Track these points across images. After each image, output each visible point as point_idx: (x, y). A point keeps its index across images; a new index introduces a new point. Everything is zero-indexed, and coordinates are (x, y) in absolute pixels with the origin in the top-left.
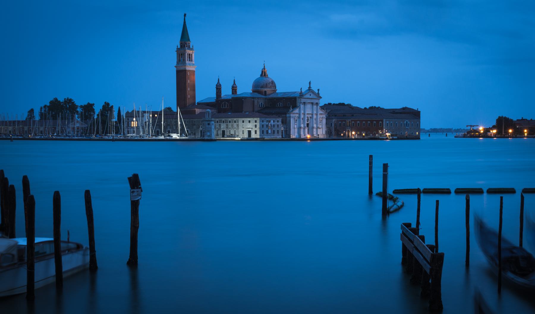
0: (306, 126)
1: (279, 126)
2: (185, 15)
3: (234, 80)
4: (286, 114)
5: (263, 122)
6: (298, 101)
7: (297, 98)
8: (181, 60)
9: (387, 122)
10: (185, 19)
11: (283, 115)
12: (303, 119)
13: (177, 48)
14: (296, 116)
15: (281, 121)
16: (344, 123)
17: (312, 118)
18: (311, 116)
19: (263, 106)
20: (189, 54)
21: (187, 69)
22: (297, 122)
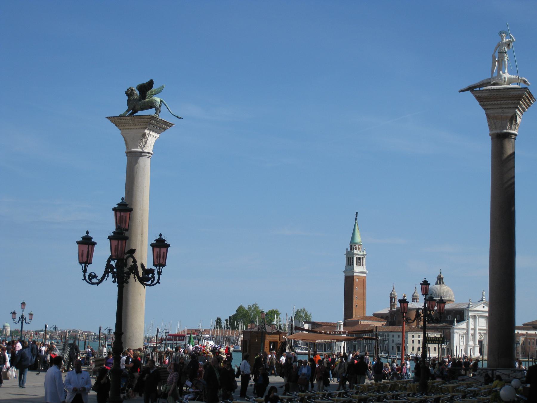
0: (477, 343)
2: (356, 214)
3: (416, 288)
4: (450, 329)
5: (413, 336)
6: (466, 314)
7: (465, 310)
8: (350, 265)
10: (356, 219)
12: (474, 335)
13: (346, 251)
16: (533, 342)
20: (359, 258)
22: (463, 339)
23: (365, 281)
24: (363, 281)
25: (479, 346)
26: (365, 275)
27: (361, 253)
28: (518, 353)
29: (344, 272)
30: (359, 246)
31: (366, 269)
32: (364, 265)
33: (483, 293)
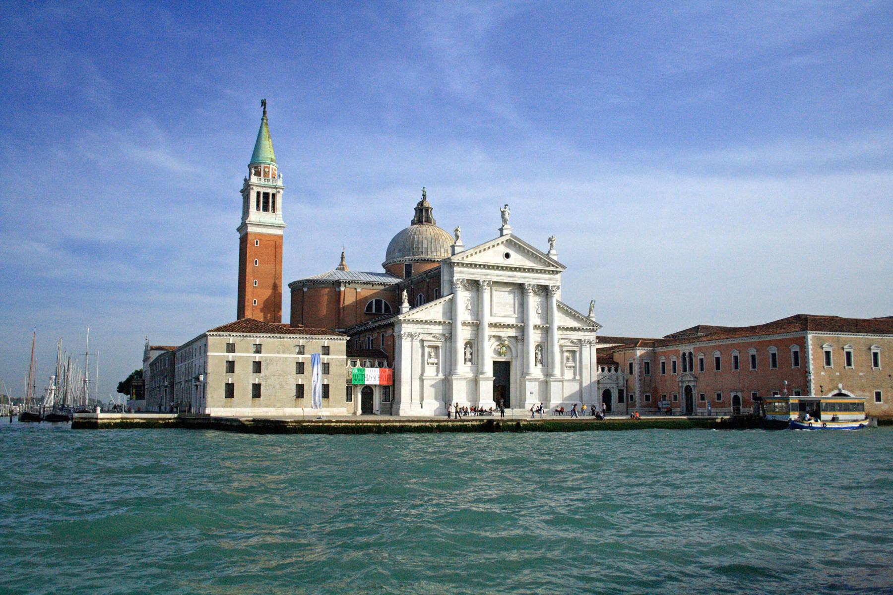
0: (488, 370)
1: (331, 369)
4: (392, 325)
5: (231, 348)
6: (445, 278)
9: (826, 348)
10: (264, 112)
11: (390, 332)
12: (474, 346)
14: (435, 332)
15: (344, 348)
17: (523, 340)
18: (512, 333)
19: (383, 312)
21: (250, 229)
22: (437, 356)
23: (281, 247)
24: (275, 246)
25: (494, 378)
26: (279, 232)
27: (271, 183)
28: (632, 397)
29: (238, 230)
30: (265, 167)
31: (283, 220)
32: (279, 211)
33: (503, 213)
